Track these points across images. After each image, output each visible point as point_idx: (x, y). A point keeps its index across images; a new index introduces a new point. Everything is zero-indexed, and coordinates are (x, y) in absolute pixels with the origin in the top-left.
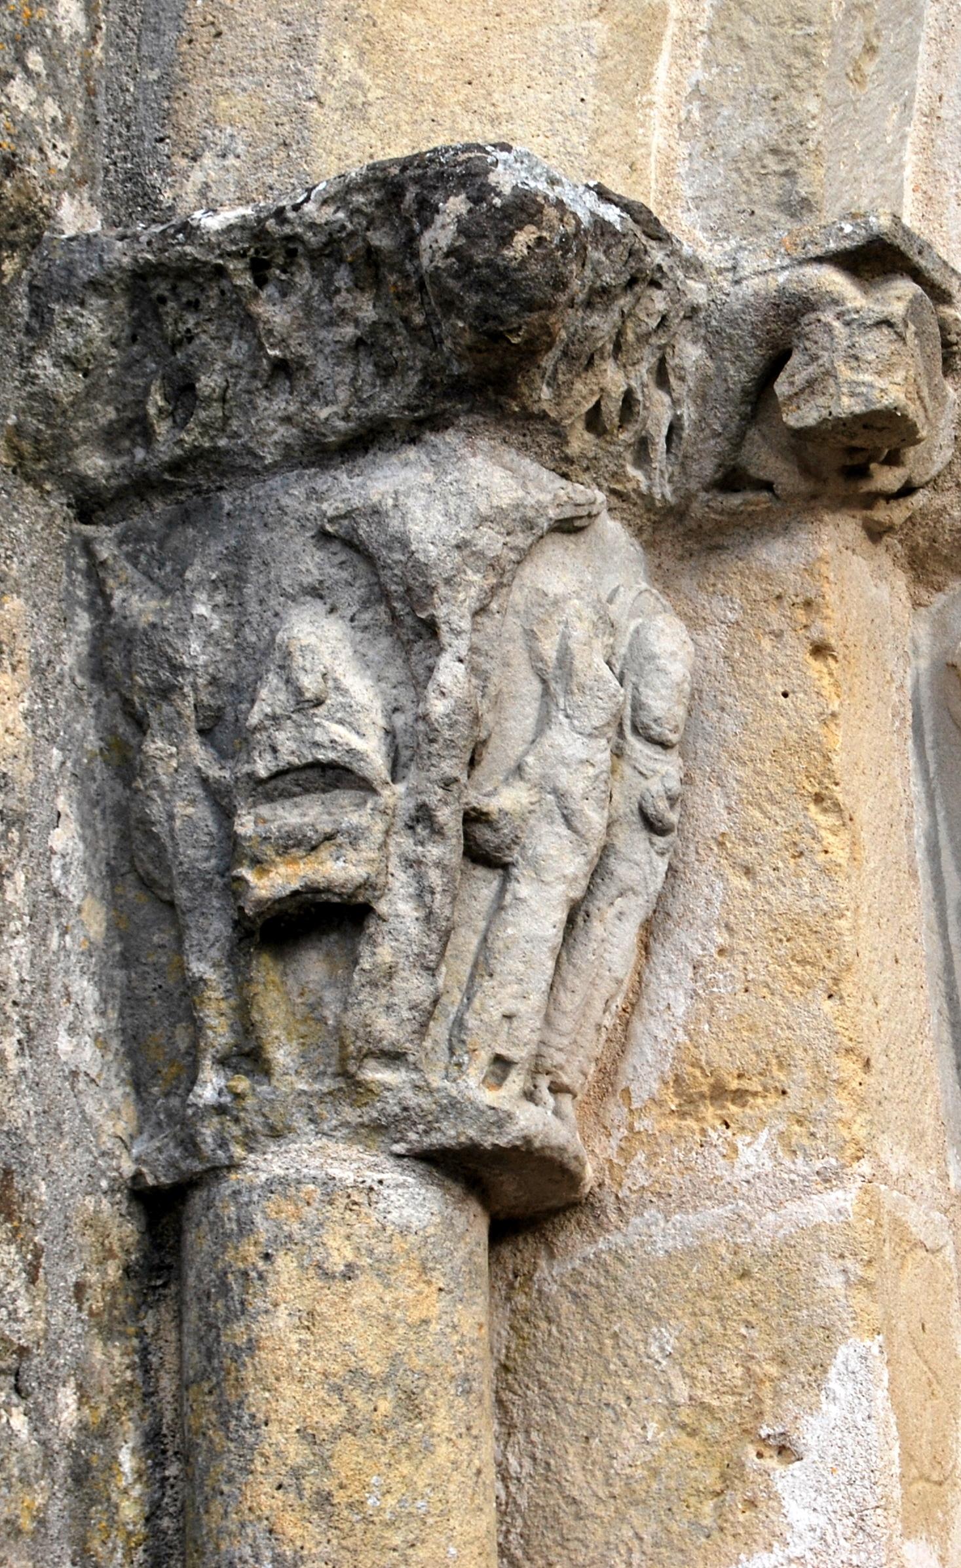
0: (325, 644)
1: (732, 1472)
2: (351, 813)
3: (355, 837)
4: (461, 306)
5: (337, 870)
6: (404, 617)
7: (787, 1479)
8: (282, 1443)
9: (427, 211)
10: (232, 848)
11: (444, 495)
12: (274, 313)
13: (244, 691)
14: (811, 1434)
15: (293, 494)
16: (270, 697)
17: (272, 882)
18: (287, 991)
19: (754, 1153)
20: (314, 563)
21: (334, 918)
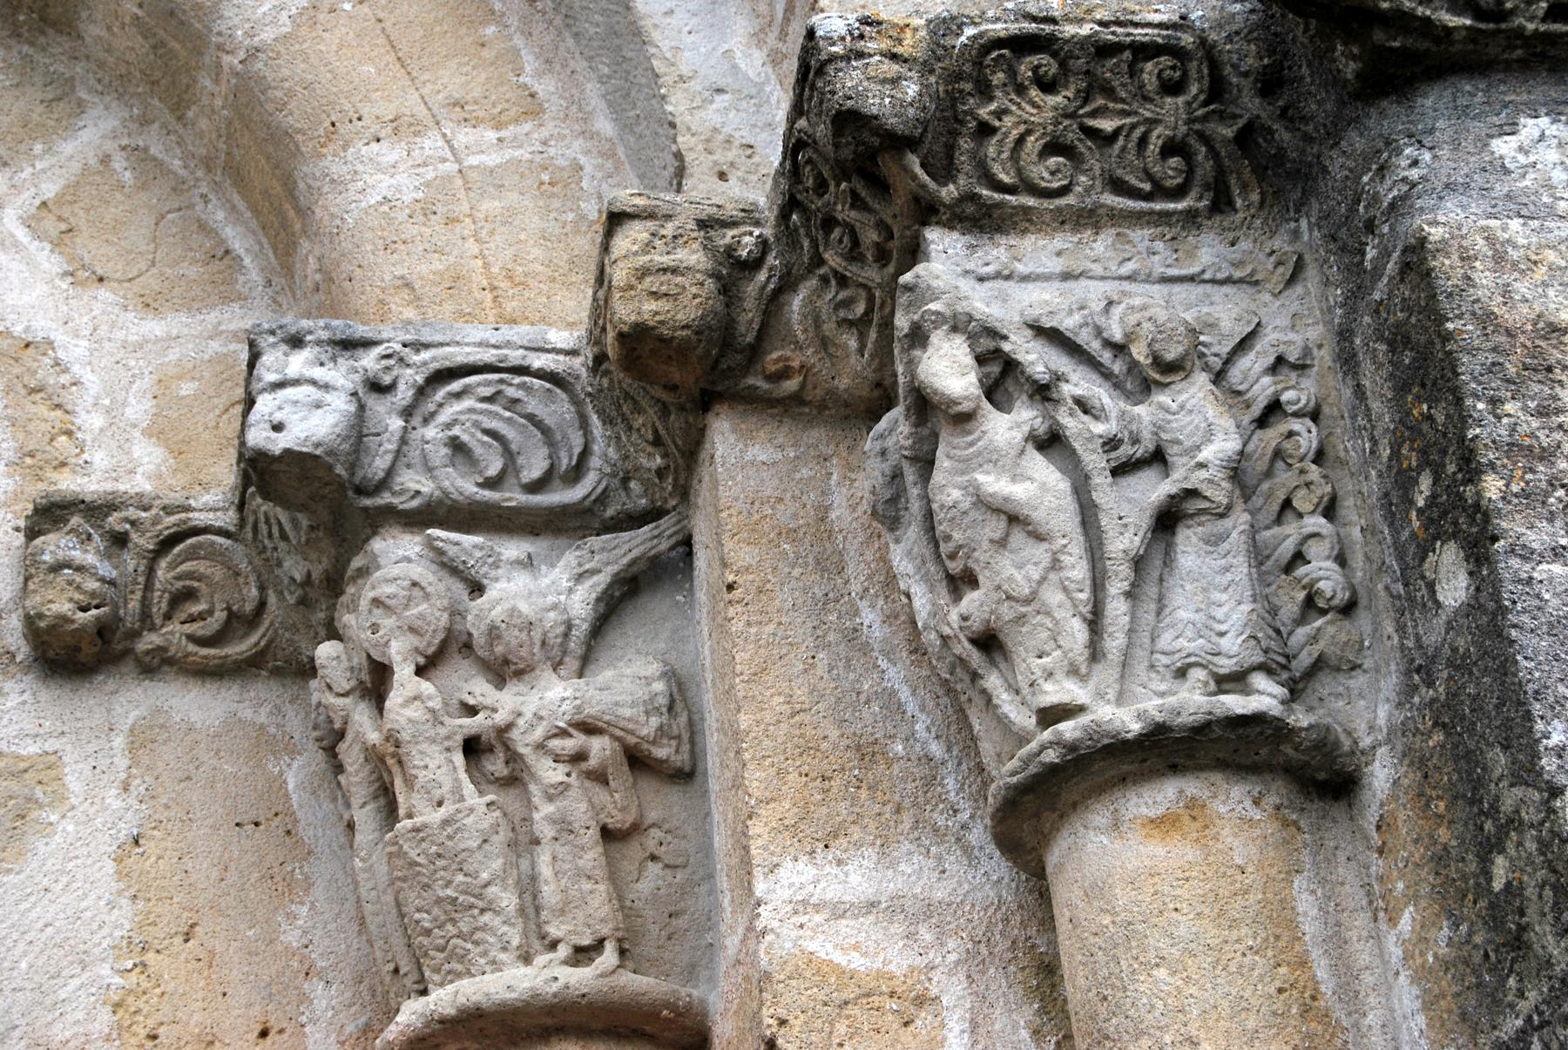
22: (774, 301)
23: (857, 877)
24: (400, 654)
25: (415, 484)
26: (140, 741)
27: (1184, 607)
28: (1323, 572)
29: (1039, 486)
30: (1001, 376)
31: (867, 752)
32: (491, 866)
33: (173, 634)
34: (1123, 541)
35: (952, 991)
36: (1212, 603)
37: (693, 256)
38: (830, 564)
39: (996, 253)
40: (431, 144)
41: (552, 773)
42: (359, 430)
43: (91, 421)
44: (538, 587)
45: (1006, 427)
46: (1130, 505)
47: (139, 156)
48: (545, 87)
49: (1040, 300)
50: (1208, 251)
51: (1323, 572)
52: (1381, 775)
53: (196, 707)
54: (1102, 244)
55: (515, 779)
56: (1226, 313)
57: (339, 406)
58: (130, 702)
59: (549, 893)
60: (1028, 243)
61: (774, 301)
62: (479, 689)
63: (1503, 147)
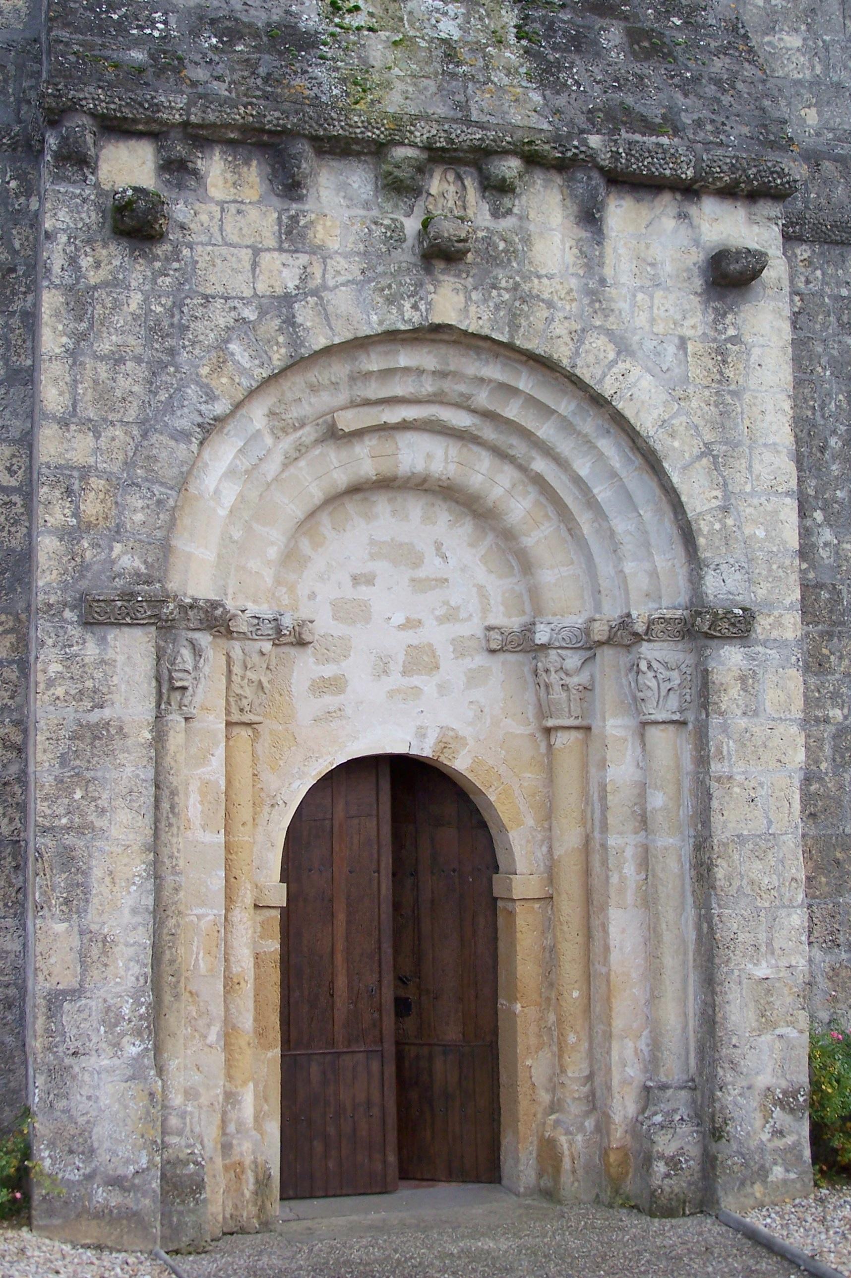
0: (186, 653)
1: (205, 757)
2: (189, 677)
3: (187, 680)
4: (215, 620)
5: (185, 684)
6: (197, 652)
7: (213, 758)
8: (171, 752)
9: (216, 608)
10: (171, 678)
11: (204, 639)
12: (190, 613)
13: (175, 659)
14: (216, 754)
15: (183, 633)
16: (179, 660)
17: (178, 684)
18: (177, 695)
19: (211, 718)
20: (185, 643)
21: (184, 688)
22: (616, 633)
23: (619, 721)
24: (552, 669)
25: (557, 644)
26: (503, 663)
27: (669, 703)
28: (688, 697)
29: (653, 684)
30: (650, 667)
31: (622, 702)
32: (565, 705)
33: (509, 647)
34: (663, 692)
35: (630, 738)
36: (673, 702)
37: (606, 628)
38: (619, 671)
39: (651, 645)
40: (556, 571)
41: (575, 692)
42: (550, 639)
43: (492, 602)
44: (573, 660)
45: (650, 674)
46: (665, 687)
47: (497, 544)
48: (574, 558)
49: (658, 655)
50: (680, 646)
51: (688, 697)
52: (690, 726)
53: (511, 657)
54: (665, 644)
55: (568, 690)
56: (681, 656)
57: (548, 635)
58: (501, 657)
59: (572, 708)
60: (656, 644)
61: (616, 633)
62: (564, 676)
63: (721, 652)
